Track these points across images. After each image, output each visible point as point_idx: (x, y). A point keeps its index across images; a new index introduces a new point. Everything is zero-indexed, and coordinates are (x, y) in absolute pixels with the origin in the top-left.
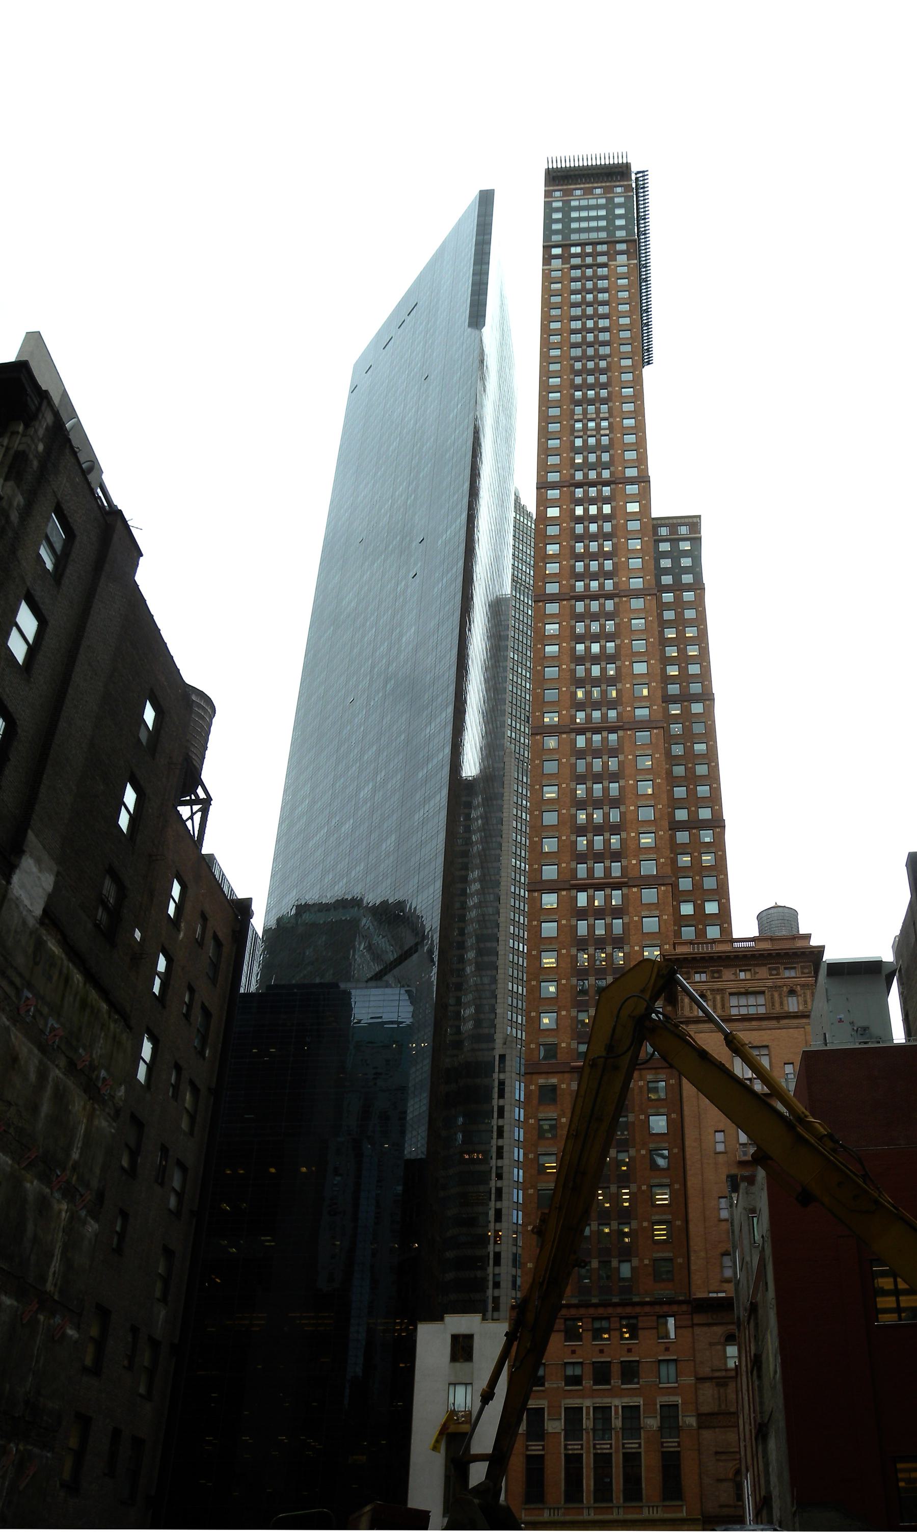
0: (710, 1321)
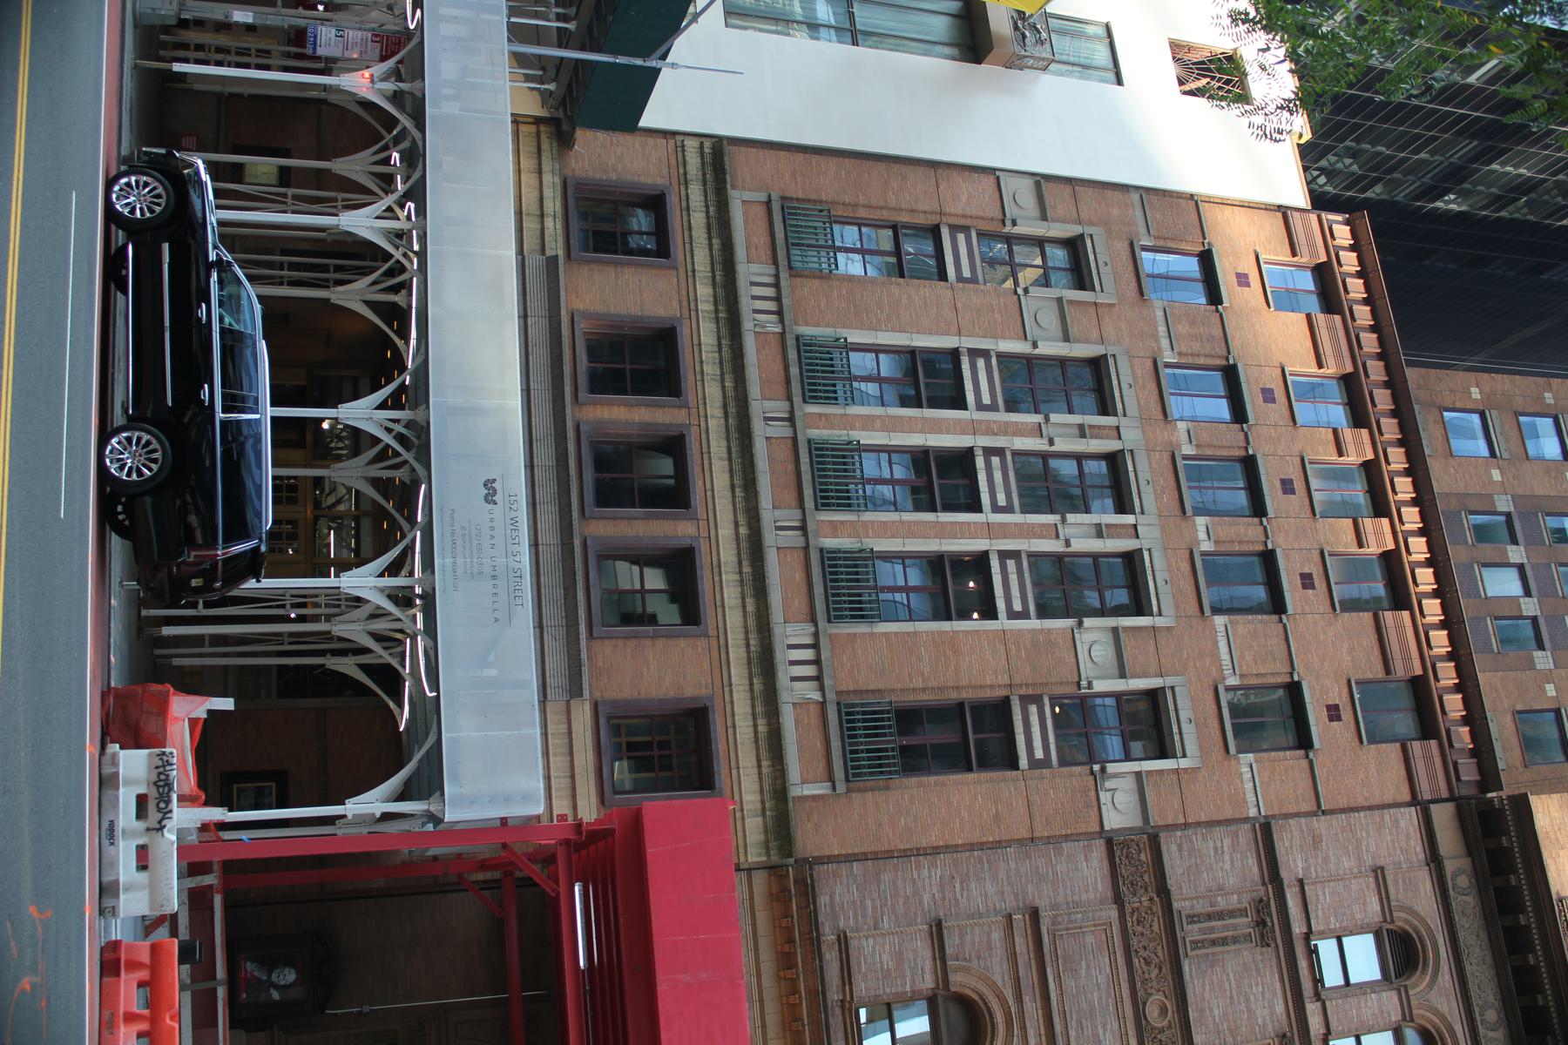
0: (1450, 866)
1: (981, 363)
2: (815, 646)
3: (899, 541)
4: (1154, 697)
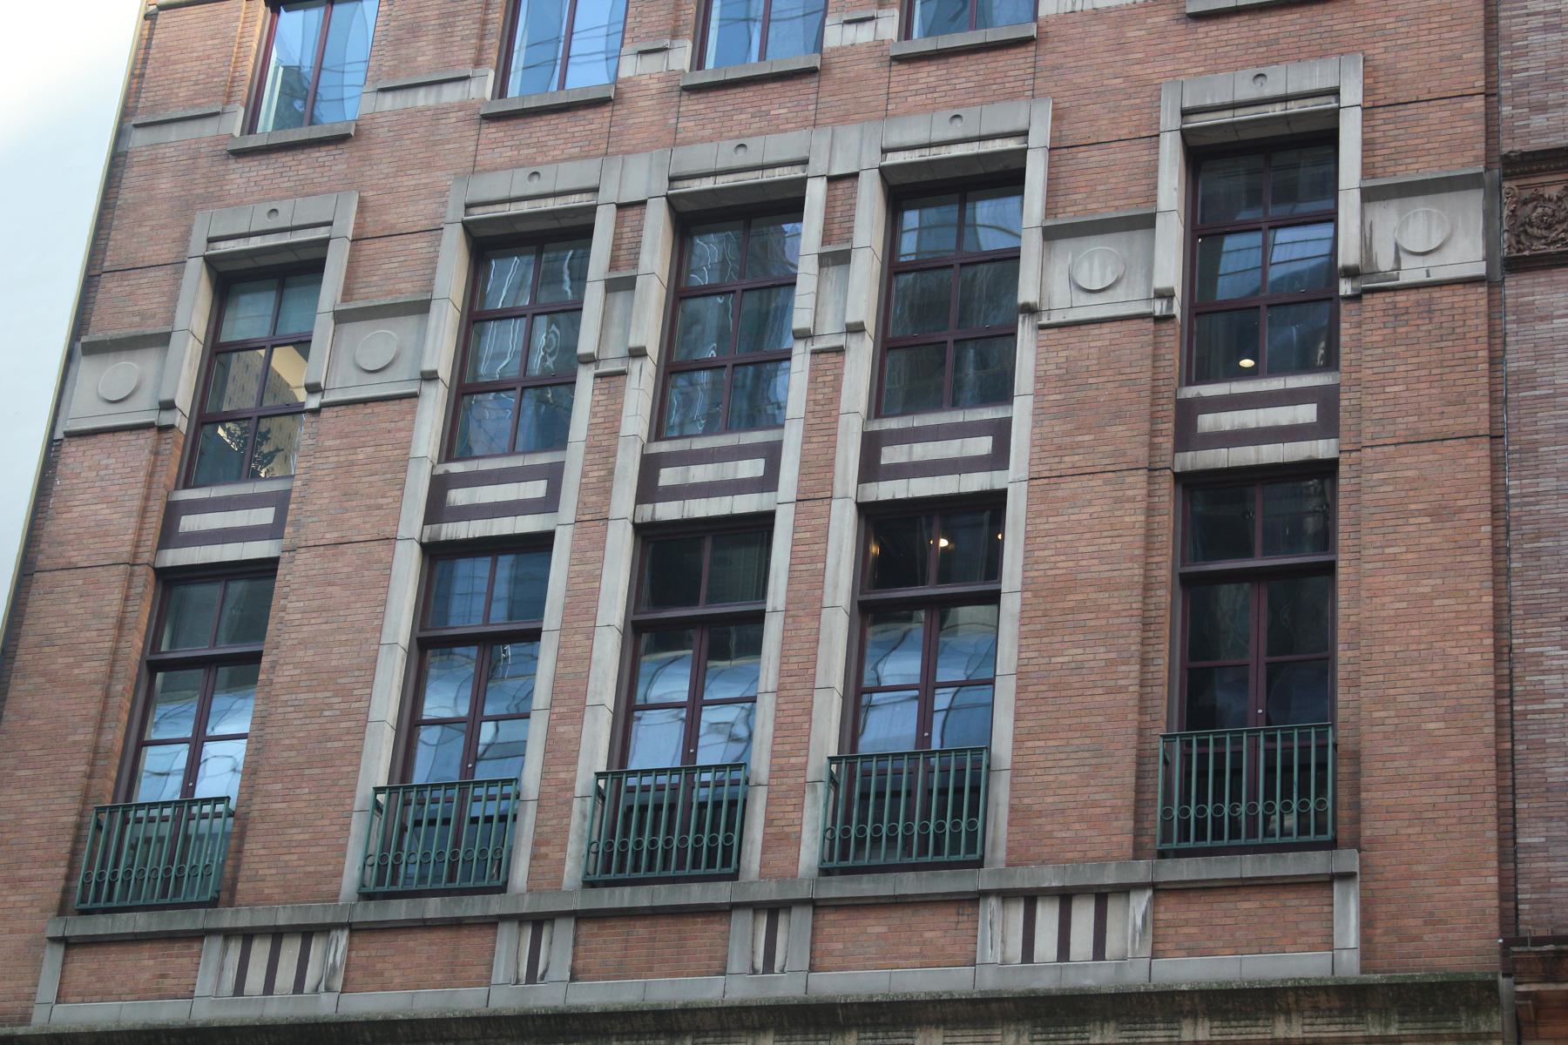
1: (458, 497)
2: (1031, 898)
3: (819, 697)
4: (1202, 154)
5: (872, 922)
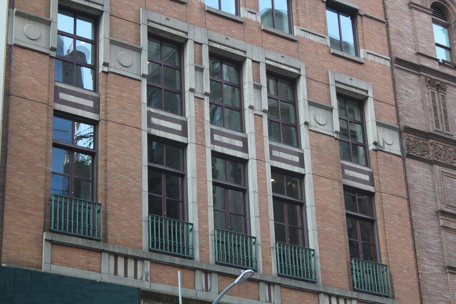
5: (294, 294)
